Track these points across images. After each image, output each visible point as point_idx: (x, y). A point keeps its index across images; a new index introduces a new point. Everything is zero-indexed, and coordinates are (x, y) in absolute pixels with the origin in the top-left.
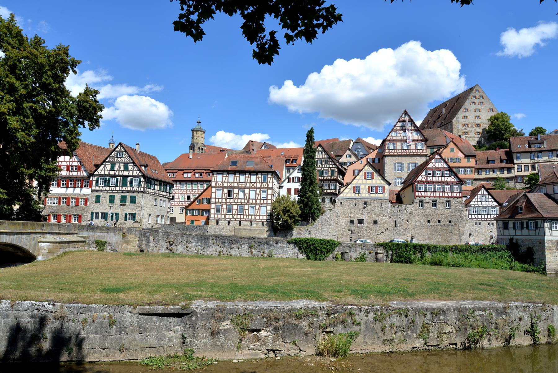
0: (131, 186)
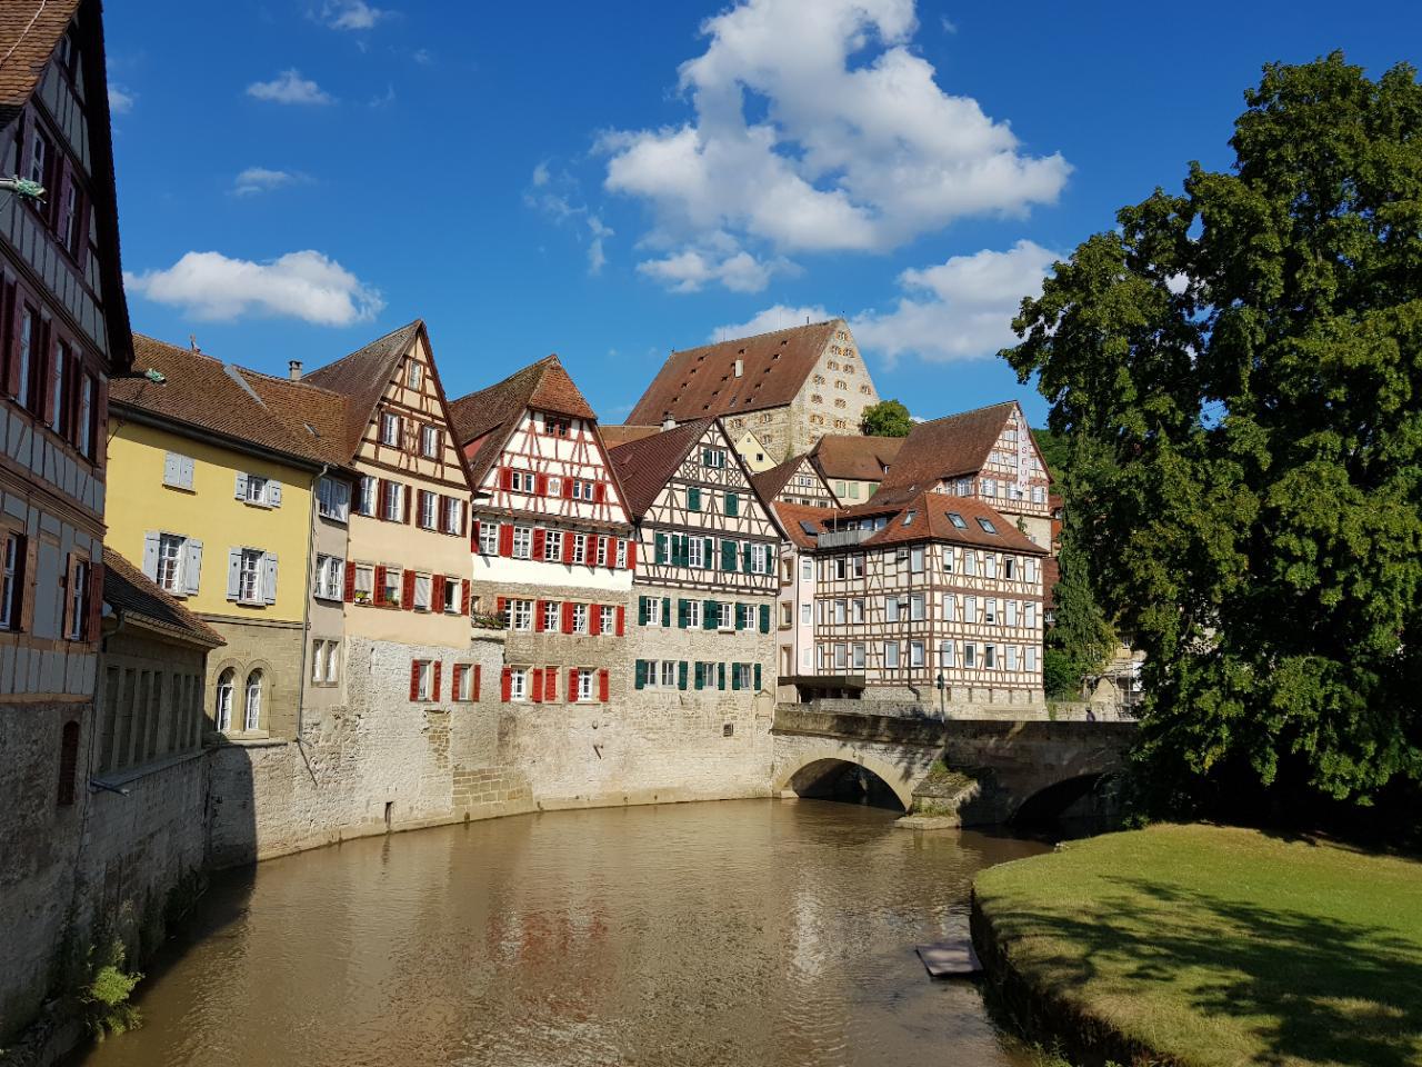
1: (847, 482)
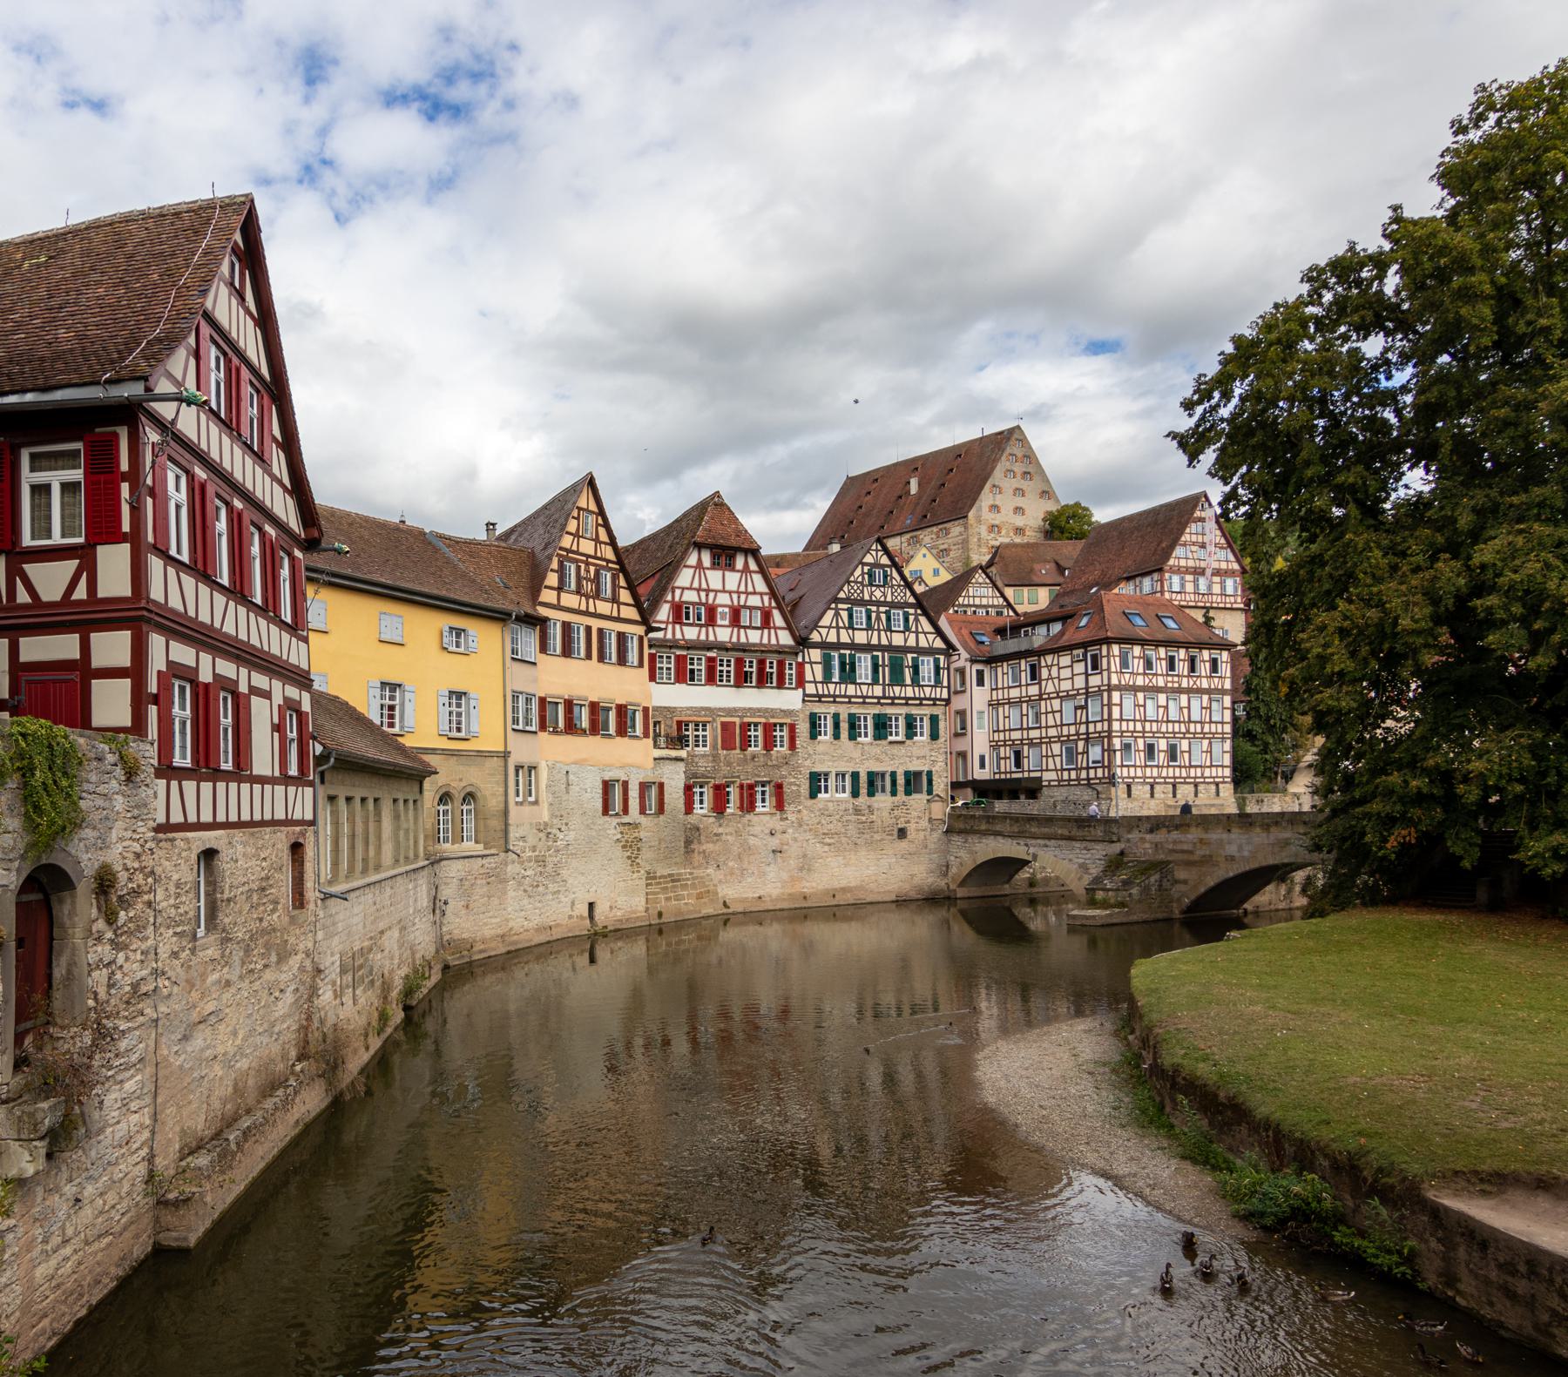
0: (916, 682)
1: (1026, 589)
